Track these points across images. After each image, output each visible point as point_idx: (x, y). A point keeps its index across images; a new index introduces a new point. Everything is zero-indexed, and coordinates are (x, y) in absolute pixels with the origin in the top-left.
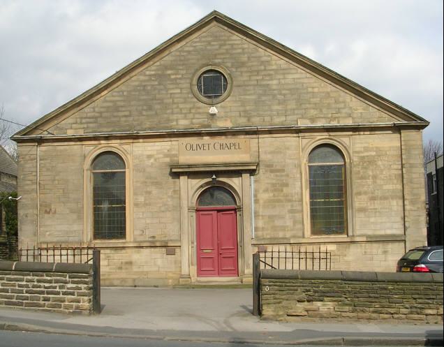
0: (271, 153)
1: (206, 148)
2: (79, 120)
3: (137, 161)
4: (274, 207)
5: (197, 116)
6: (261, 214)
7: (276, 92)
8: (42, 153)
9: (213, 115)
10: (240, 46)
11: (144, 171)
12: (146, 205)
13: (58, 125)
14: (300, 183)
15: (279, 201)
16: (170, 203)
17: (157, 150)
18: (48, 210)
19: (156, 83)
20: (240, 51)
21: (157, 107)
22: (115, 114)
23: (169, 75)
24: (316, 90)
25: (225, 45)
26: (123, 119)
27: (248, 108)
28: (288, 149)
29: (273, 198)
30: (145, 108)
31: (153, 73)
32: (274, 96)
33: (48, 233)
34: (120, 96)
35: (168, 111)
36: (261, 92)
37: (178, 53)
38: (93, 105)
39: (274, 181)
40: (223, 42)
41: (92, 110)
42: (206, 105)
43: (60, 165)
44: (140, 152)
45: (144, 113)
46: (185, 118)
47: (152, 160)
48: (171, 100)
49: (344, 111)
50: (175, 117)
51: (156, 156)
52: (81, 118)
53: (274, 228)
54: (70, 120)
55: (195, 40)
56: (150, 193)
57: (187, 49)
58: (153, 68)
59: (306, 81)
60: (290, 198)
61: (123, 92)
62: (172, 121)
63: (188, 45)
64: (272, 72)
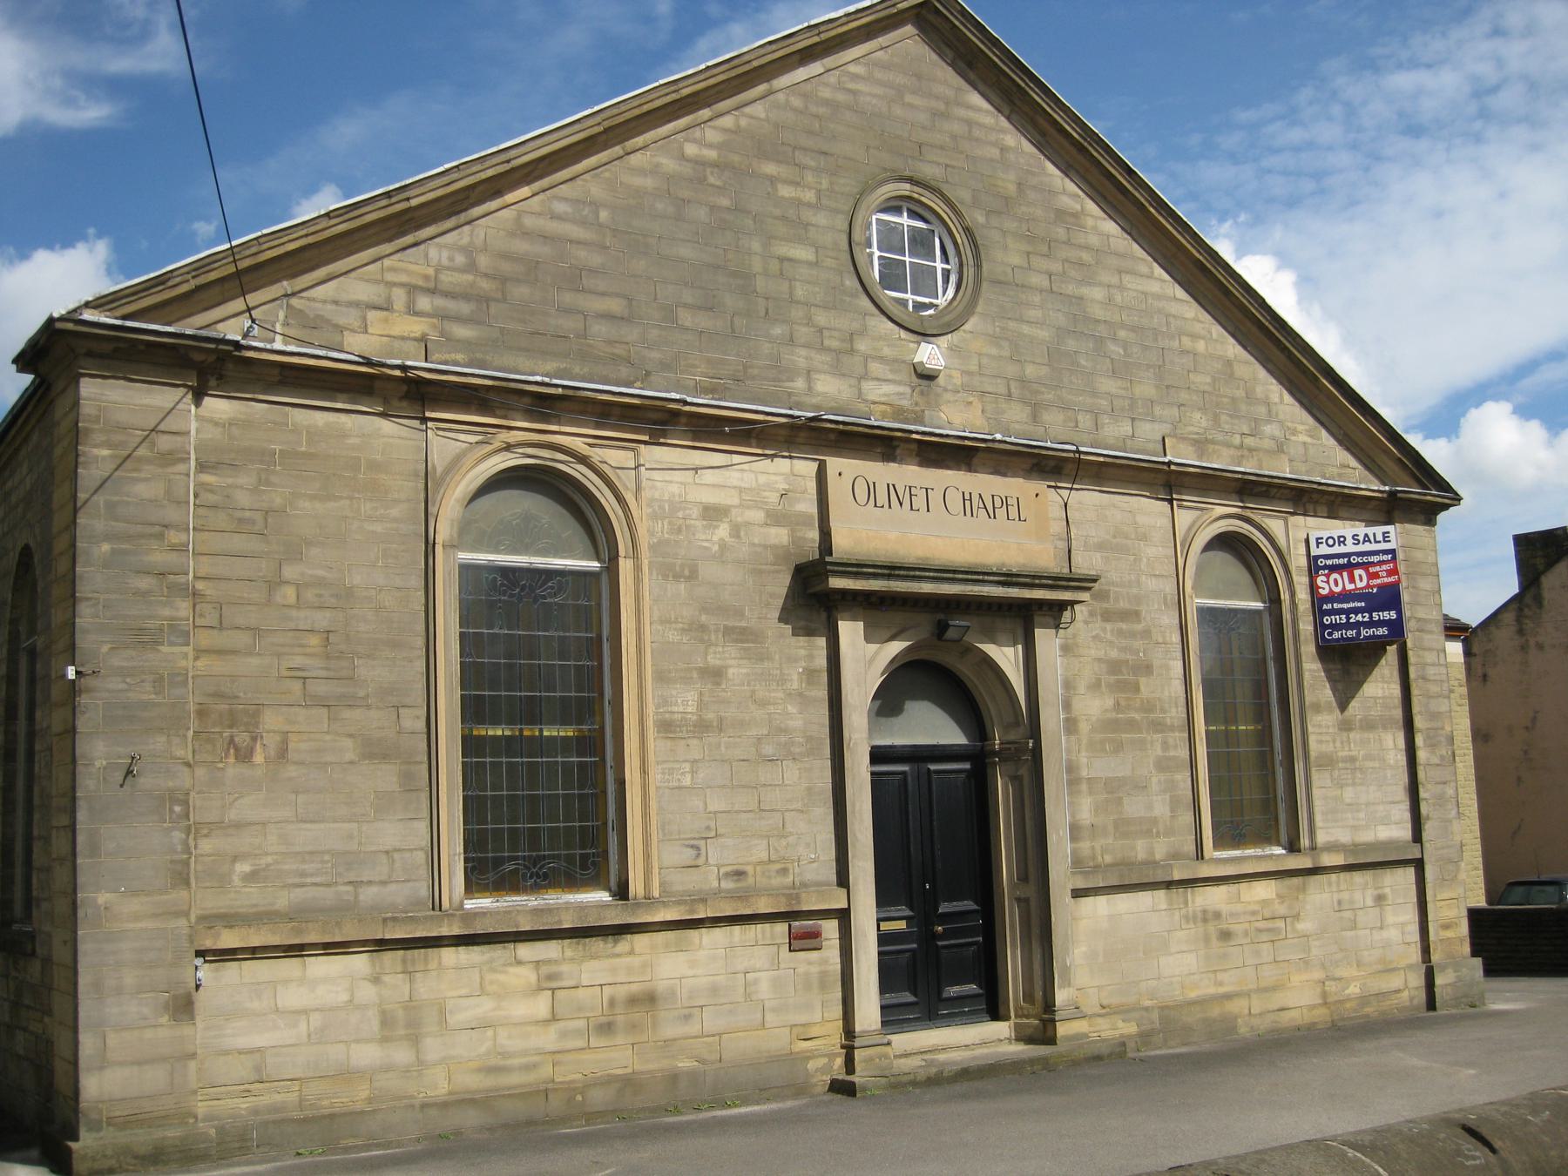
0: (1100, 547)
1: (920, 502)
2: (399, 297)
3: (663, 528)
4: (1118, 748)
5: (876, 368)
6: (1084, 773)
7: (1102, 330)
8: (212, 433)
9: (927, 376)
10: (993, 137)
11: (692, 575)
12: (702, 727)
13: (294, 301)
14: (1180, 664)
15: (1132, 725)
16: (796, 723)
17: (741, 490)
18: (242, 738)
19: (725, 202)
20: (994, 153)
21: (730, 301)
22: (568, 298)
23: (773, 180)
24: (1201, 346)
25: (945, 116)
26: (600, 329)
27: (1030, 371)
28: (1144, 538)
29: (1114, 715)
30: (688, 296)
31: (712, 154)
32: (1099, 341)
33: (243, 867)
34: (583, 223)
35: (777, 331)
36: (1062, 320)
37: (797, 102)
38: (463, 236)
39: (1114, 654)
40: (942, 107)
41: (460, 259)
42: (903, 334)
43: (305, 504)
44: (675, 489)
45: (686, 318)
46: (838, 371)
47: (723, 531)
48: (785, 286)
49: (1269, 429)
50: (800, 357)
51: (739, 516)
52: (412, 289)
53: (1124, 828)
54: (358, 288)
55: (852, 68)
56: (715, 675)
57: (826, 93)
58: (711, 135)
59: (1174, 308)
60: (1157, 715)
61: (596, 206)
62: (792, 374)
63: (832, 78)
64: (1086, 257)
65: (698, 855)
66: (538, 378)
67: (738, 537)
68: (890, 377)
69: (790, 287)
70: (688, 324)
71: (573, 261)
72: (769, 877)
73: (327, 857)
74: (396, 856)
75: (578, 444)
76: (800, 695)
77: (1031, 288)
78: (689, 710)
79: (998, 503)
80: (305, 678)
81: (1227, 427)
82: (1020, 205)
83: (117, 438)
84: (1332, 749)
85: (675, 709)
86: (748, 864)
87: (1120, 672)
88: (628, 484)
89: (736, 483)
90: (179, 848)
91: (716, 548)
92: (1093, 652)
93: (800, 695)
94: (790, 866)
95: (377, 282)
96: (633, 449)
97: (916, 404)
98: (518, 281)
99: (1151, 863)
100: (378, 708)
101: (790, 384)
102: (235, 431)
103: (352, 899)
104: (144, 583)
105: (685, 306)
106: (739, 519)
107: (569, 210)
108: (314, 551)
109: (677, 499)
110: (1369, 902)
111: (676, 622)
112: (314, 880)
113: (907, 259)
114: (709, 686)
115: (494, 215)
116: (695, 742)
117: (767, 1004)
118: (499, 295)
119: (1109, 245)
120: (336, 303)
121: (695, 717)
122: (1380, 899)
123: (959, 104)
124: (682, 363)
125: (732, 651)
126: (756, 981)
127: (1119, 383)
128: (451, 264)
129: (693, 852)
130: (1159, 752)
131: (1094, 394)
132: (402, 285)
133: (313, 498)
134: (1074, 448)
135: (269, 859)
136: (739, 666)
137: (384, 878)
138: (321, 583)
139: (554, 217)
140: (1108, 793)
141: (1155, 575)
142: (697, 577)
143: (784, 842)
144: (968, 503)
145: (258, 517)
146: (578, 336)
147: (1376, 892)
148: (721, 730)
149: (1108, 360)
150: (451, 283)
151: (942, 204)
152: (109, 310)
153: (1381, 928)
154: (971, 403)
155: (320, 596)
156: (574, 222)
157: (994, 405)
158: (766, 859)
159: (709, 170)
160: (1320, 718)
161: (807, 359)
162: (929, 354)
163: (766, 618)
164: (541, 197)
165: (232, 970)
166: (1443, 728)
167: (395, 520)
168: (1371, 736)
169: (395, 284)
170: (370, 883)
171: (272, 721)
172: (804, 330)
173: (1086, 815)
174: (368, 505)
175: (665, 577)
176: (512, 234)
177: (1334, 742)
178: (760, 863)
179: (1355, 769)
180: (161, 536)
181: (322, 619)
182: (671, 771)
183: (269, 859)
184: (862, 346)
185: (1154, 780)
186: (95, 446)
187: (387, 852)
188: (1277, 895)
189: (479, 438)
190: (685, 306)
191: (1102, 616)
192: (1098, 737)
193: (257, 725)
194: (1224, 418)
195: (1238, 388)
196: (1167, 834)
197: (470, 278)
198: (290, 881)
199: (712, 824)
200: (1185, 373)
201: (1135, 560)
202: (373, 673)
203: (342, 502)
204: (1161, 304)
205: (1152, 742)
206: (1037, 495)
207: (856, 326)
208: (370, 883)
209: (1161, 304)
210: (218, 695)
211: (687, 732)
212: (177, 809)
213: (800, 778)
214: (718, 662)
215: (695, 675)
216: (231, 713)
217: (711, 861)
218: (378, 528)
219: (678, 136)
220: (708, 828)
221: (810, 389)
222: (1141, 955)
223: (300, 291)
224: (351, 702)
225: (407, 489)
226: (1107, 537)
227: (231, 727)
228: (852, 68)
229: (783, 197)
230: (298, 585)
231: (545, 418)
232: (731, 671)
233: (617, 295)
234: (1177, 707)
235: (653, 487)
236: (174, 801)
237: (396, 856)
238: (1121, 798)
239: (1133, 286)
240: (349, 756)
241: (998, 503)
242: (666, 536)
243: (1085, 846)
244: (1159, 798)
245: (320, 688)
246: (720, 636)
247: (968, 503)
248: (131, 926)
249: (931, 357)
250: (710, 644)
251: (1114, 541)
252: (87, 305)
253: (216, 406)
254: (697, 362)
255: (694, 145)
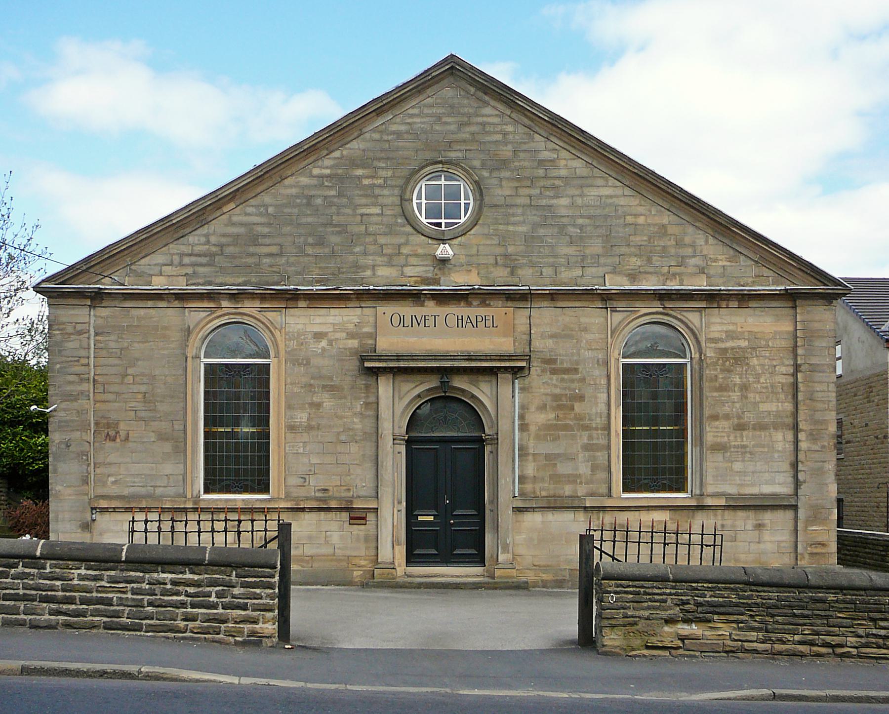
0: (553, 336)
1: (429, 323)
2: (176, 259)
3: (293, 344)
4: (556, 438)
5: (413, 260)
6: (531, 451)
7: (565, 221)
8: (100, 321)
9: (444, 261)
10: (499, 128)
11: (308, 363)
12: (310, 428)
13: (133, 267)
14: (605, 395)
15: (566, 427)
16: (359, 426)
17: (334, 324)
18: (112, 433)
19: (333, 193)
20: (499, 137)
21: (334, 239)
22: (252, 249)
23: (359, 178)
24: (641, 220)
25: (469, 124)
26: (267, 260)
27: (511, 249)
28: (585, 330)
29: (555, 422)
30: (310, 240)
31: (328, 171)
32: (562, 228)
33: (112, 479)
34: (260, 215)
35: (357, 249)
36: (537, 219)
37: (376, 136)
38: (204, 230)
39: (557, 391)
40: (466, 119)
41: (203, 239)
42: (430, 241)
43: (136, 345)
44: (300, 327)
45: (310, 250)
46: (390, 264)
47: (324, 343)
48: (363, 228)
49: (693, 261)
50: (369, 260)
51: (331, 336)
52: (182, 255)
53: (556, 478)
54: (159, 258)
55: (411, 111)
56: (318, 405)
57: (394, 128)
58: (327, 162)
59: (622, 201)
60: (587, 422)
61: (266, 206)
62: (364, 268)
63: (398, 120)
64: (557, 182)
65: (305, 482)
66: (226, 287)
67: (332, 345)
68: (421, 263)
69: (366, 227)
70: (310, 252)
71: (255, 233)
72: (340, 492)
73: (143, 476)
74: (171, 477)
75: (254, 312)
76: (361, 414)
77: (516, 205)
78: (303, 421)
79: (479, 319)
80: (136, 410)
81: (658, 264)
82: (513, 162)
83: (61, 327)
84: (727, 440)
85: (296, 420)
86: (330, 486)
87: (561, 400)
88: (277, 326)
89: (331, 321)
90: (85, 471)
91: (320, 351)
92: (542, 390)
93: (361, 414)
94: (351, 488)
95: (167, 254)
96: (280, 311)
97: (436, 275)
98: (229, 245)
99: (574, 497)
100: (165, 421)
101: (364, 273)
102: (109, 320)
103: (152, 492)
104: (71, 378)
105: (309, 244)
106: (333, 338)
107: (254, 210)
108: (140, 363)
109: (301, 331)
110: (749, 527)
111: (298, 384)
112: (138, 484)
113: (443, 202)
114: (314, 410)
115: (219, 218)
116: (305, 434)
117: (337, 546)
118: (220, 253)
119: (576, 173)
120: (149, 265)
121: (306, 424)
122: (759, 526)
123: (477, 116)
124: (306, 271)
125: (326, 395)
126: (331, 536)
127: (575, 248)
128: (199, 243)
129: (302, 480)
130: (586, 441)
131: (556, 256)
132: (177, 254)
133: (139, 342)
134: (528, 288)
135: (121, 476)
136: (329, 402)
137: (166, 485)
138: (142, 374)
139: (249, 215)
140: (546, 460)
141: (591, 349)
142: (310, 364)
143: (348, 478)
144: (460, 321)
145: (118, 351)
146: (256, 265)
147: (755, 522)
148: (318, 429)
149: (567, 237)
150: (199, 250)
151: (461, 171)
152: (54, 281)
153: (759, 542)
154: (471, 270)
155: (142, 379)
156: (256, 215)
157: (486, 270)
158: (339, 484)
159: (325, 179)
160: (717, 423)
161: (373, 260)
162: (444, 250)
163: (344, 380)
164: (241, 206)
165: (107, 516)
166: (827, 429)
167: (174, 349)
168: (763, 434)
169: (174, 254)
170: (160, 486)
171: (122, 426)
172: (372, 247)
173: (530, 470)
174: (162, 344)
175: (294, 365)
176: (226, 225)
177: (728, 437)
178: (336, 486)
179: (746, 452)
180: (78, 361)
181: (143, 388)
182: (293, 446)
183: (121, 476)
184: (405, 250)
185: (581, 455)
186: (54, 330)
187: (167, 475)
188: (670, 518)
189: (209, 313)
190: (309, 244)
191: (550, 372)
192: (542, 433)
193: (117, 428)
194: (654, 258)
195: (670, 240)
196: (587, 483)
197: (207, 247)
198: (129, 485)
199: (313, 469)
200: (628, 236)
201: (577, 342)
202: (163, 407)
203: (151, 343)
204: (611, 201)
205: (581, 436)
206: (506, 313)
207: (402, 240)
208: (160, 486)
209: (611, 201)
210: (103, 417)
211: (302, 430)
212: (84, 457)
213: (359, 450)
214: (318, 400)
215: (307, 406)
216: (108, 423)
217: (311, 484)
218: (165, 352)
219: (309, 166)
220: (310, 470)
221: (374, 274)
222: (564, 542)
223: (135, 262)
224: (154, 419)
225: (176, 336)
226: (558, 331)
227: (108, 428)
228: (411, 111)
229: (365, 185)
230: (133, 376)
231: (238, 302)
232: (325, 404)
233: (275, 245)
234: (601, 417)
235: (290, 327)
236: (83, 455)
237: (171, 477)
238: (556, 464)
239: (592, 193)
240: (153, 439)
241: (479, 319)
242: (295, 347)
243: (529, 487)
244: (584, 464)
245: (143, 414)
246: (320, 389)
247: (460, 321)
248: (67, 497)
249: (443, 251)
250: (315, 392)
251: (563, 333)
252: (43, 281)
253: (103, 312)
254: (314, 269)
255: (318, 169)
